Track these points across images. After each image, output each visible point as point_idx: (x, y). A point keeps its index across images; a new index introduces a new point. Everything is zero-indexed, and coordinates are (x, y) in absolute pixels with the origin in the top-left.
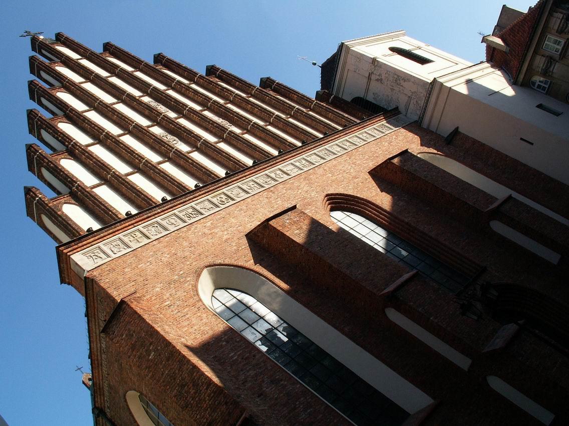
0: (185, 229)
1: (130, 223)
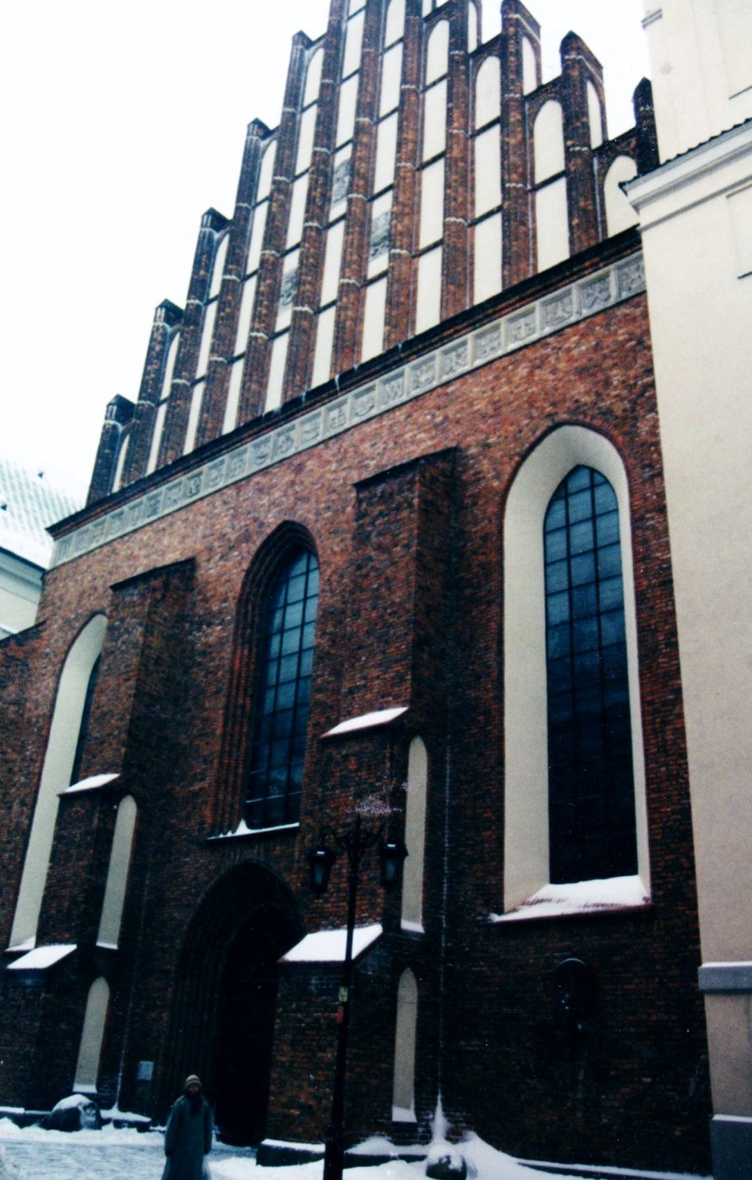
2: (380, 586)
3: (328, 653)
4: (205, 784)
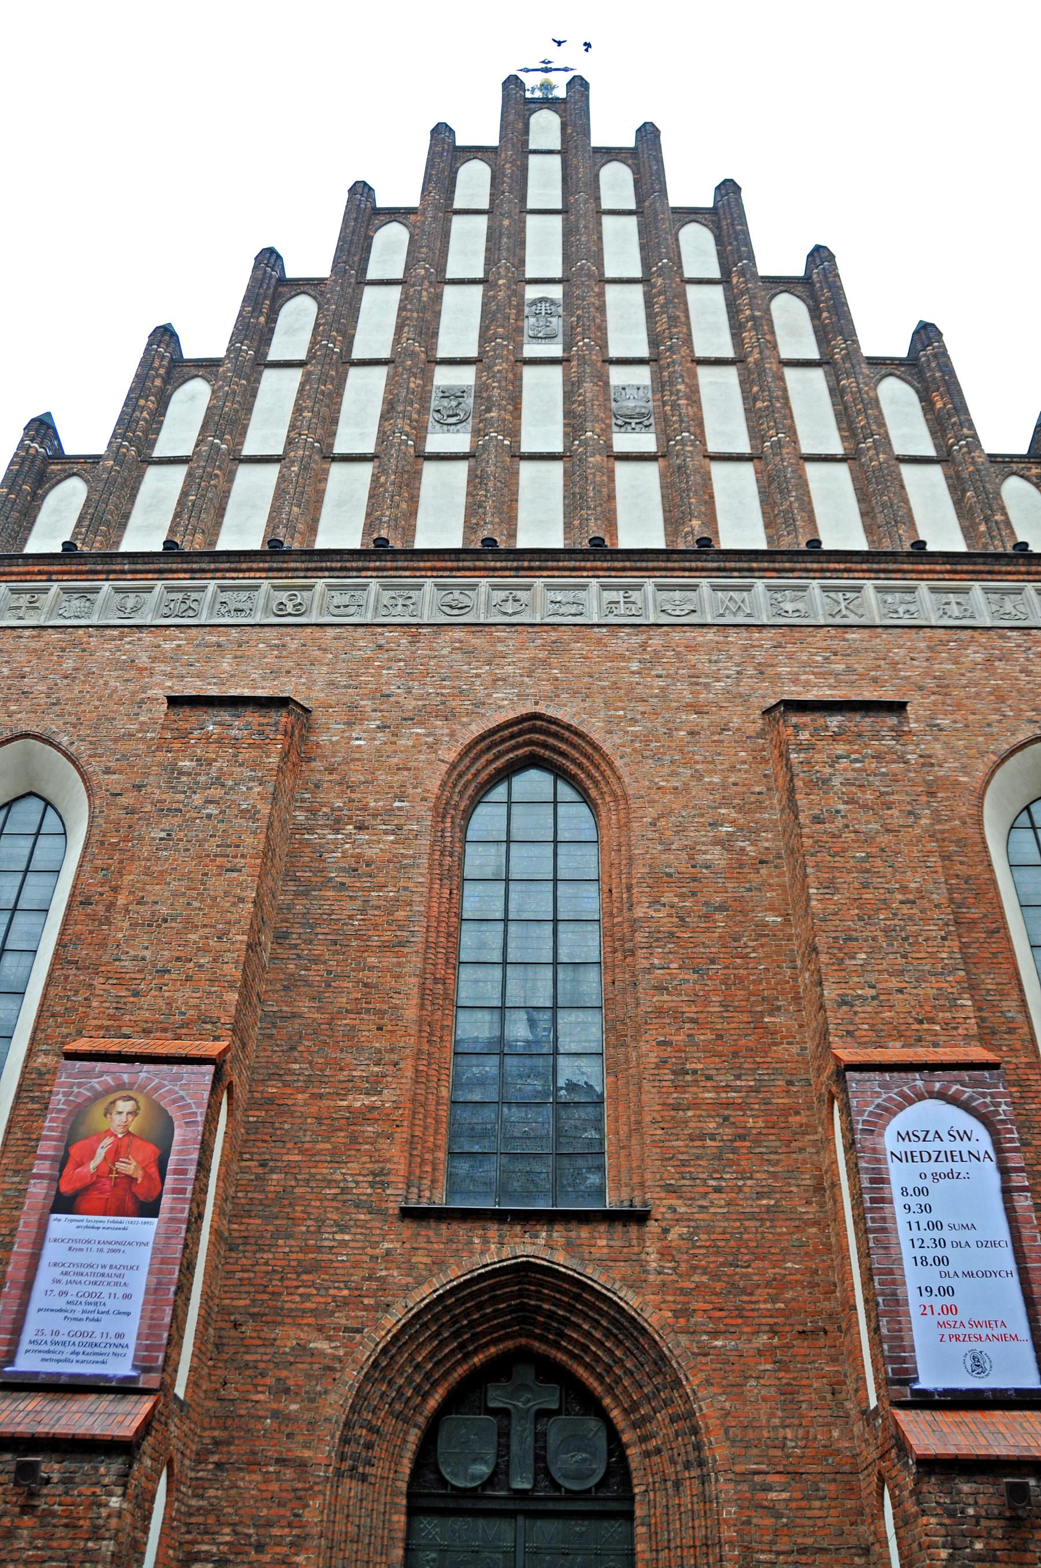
0: (116, 633)
1: (46, 568)
2: (869, 856)
3: (672, 934)
4: (388, 1097)
